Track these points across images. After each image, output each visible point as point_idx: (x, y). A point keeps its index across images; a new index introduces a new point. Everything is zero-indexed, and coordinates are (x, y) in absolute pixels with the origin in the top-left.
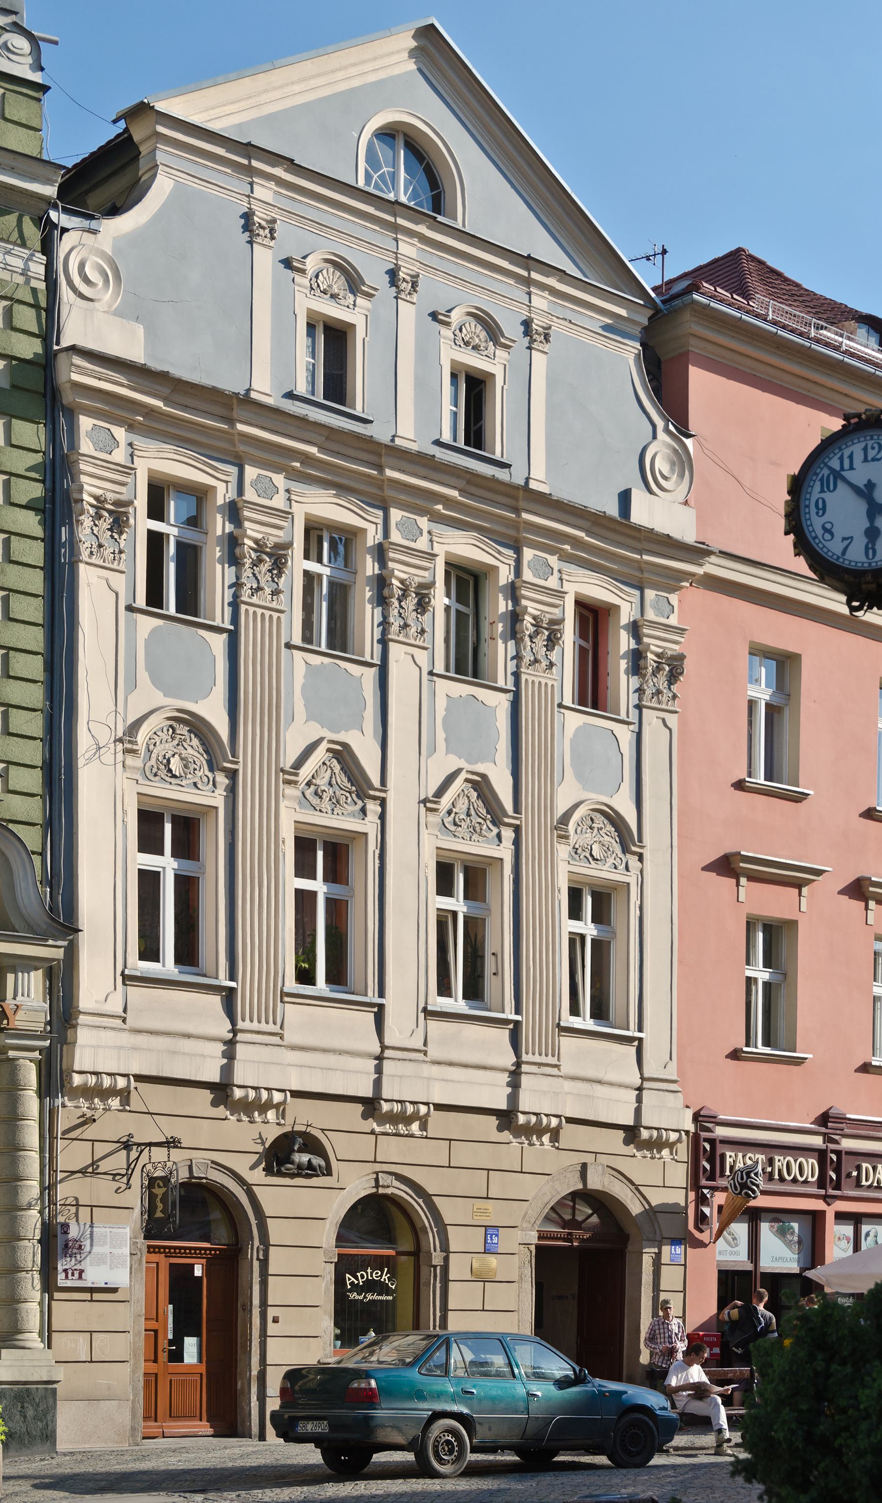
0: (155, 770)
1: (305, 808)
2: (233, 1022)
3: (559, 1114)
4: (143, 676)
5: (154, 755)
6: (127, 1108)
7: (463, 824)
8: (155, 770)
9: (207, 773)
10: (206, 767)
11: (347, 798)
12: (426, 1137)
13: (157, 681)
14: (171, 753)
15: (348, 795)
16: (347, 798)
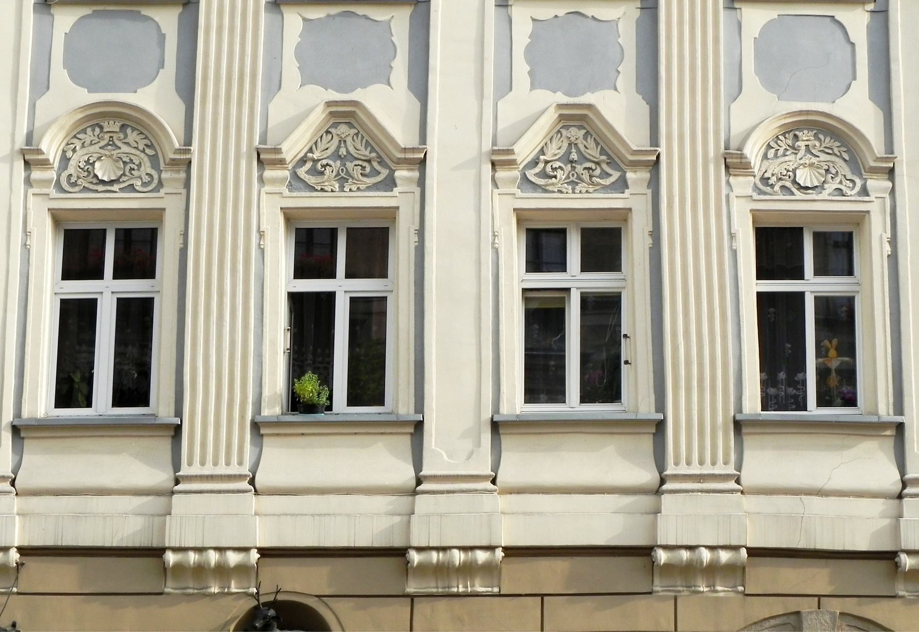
0: (73, 180)
1: (299, 190)
2: (177, 466)
3: (734, 543)
4: (59, 74)
5: (73, 163)
6: (15, 590)
7: (559, 173)
8: (73, 180)
9: (150, 170)
10: (148, 164)
11: (363, 168)
12: (500, 595)
13: (77, 78)
14: (96, 156)
15: (365, 164)
16: (363, 168)
